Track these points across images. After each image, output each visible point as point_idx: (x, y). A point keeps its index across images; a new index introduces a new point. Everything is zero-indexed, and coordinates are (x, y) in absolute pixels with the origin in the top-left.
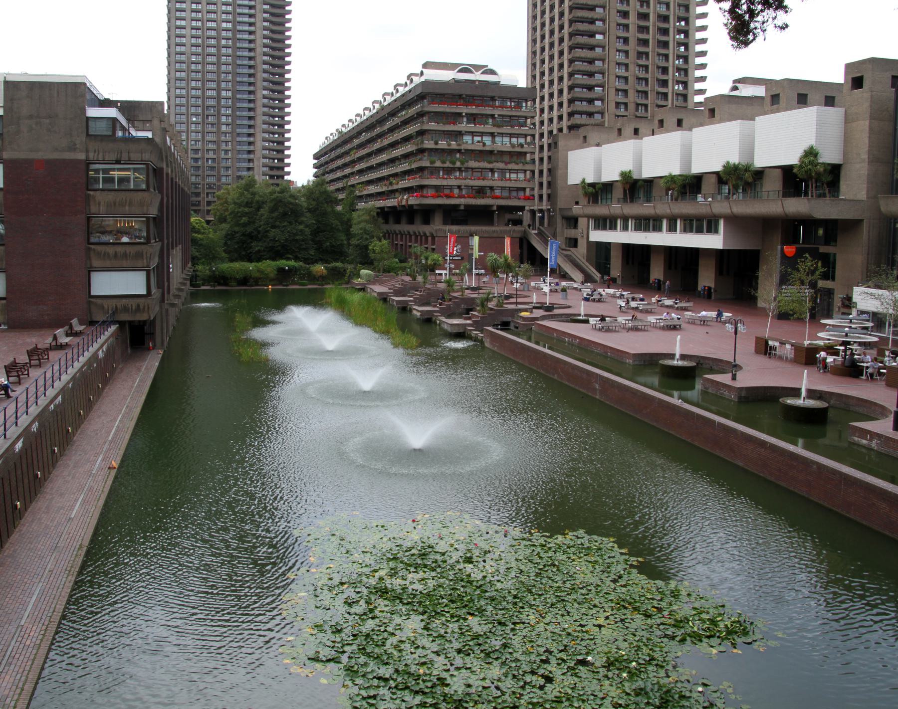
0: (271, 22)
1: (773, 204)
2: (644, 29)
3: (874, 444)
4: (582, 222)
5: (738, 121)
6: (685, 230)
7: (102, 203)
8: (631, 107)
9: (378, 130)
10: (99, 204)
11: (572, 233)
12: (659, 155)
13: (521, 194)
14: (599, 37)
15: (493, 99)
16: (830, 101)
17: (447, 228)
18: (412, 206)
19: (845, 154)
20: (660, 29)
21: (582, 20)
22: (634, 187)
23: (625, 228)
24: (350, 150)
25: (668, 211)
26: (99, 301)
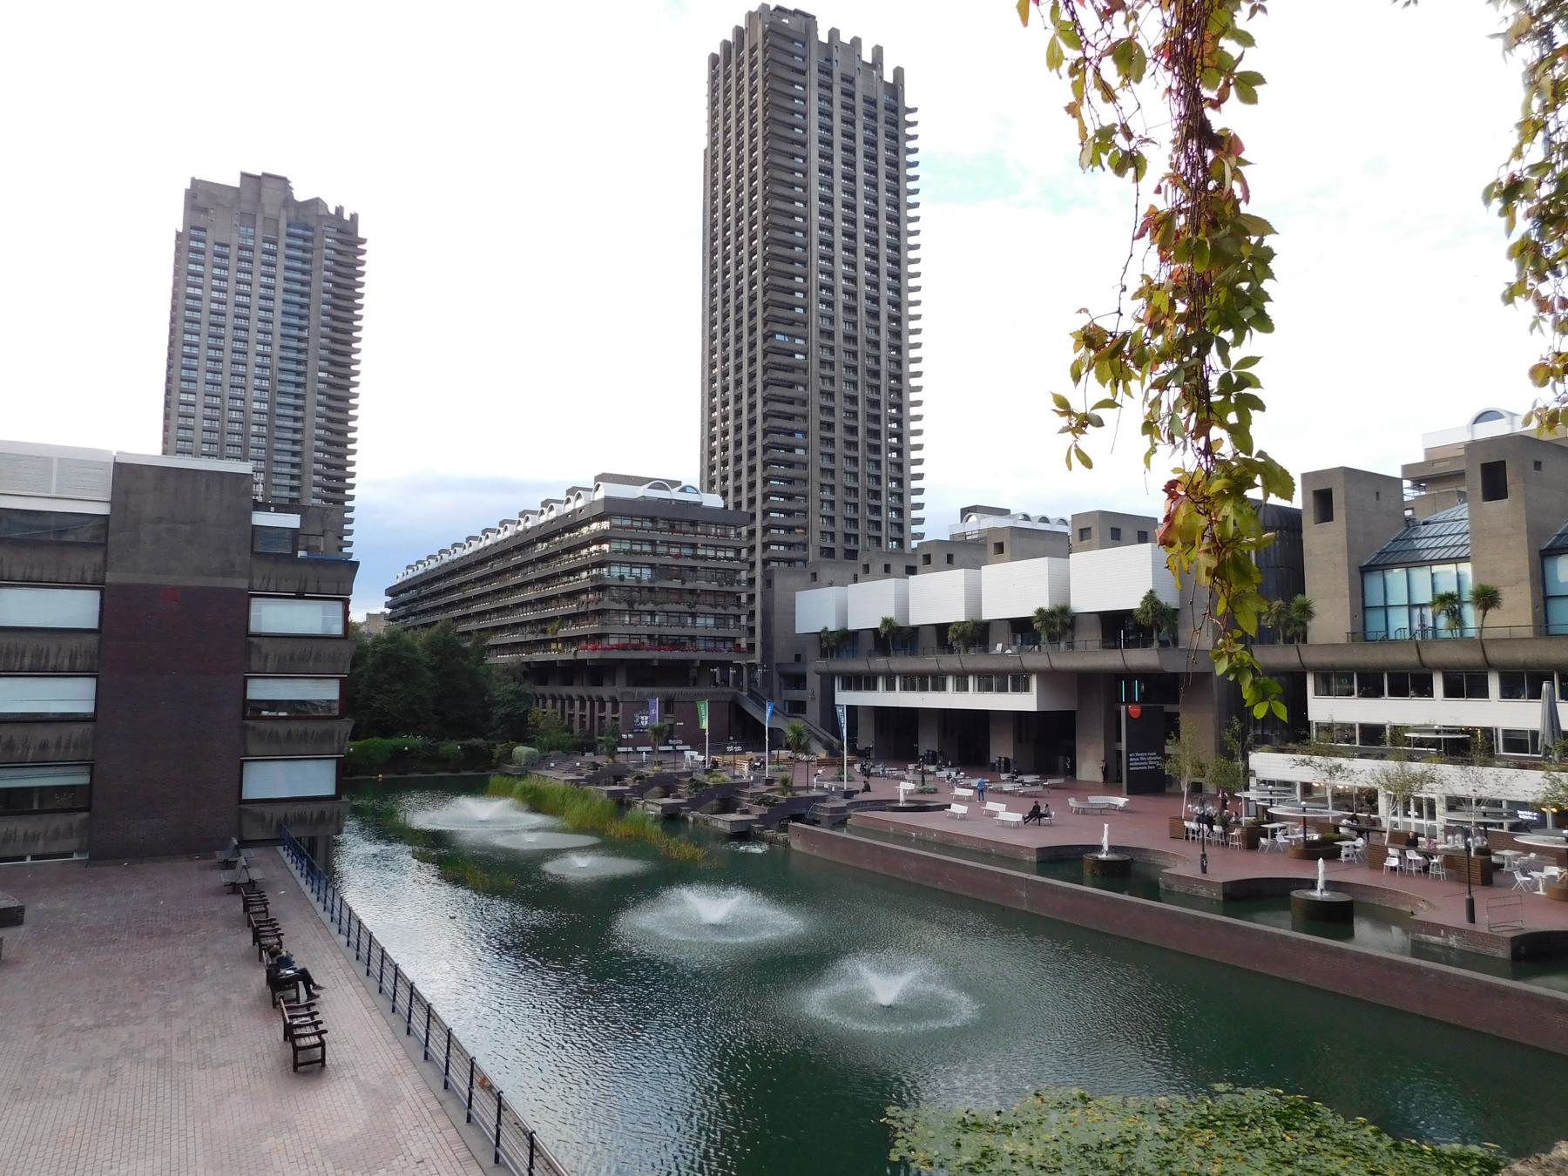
0: (329, 407)
1: (1093, 656)
2: (852, 445)
3: (1452, 941)
4: (814, 682)
5: (1045, 560)
6: (905, 688)
7: (271, 656)
8: (839, 537)
9: (517, 559)
10: (266, 657)
11: (796, 695)
12: (937, 598)
13: (729, 645)
14: (799, 452)
15: (694, 523)
16: (1143, 537)
17: (637, 690)
18: (585, 661)
19: (1182, 599)
20: (870, 446)
21: (778, 431)
22: (896, 636)
23: (890, 687)
24: (461, 585)
25: (959, 666)
26: (258, 809)
